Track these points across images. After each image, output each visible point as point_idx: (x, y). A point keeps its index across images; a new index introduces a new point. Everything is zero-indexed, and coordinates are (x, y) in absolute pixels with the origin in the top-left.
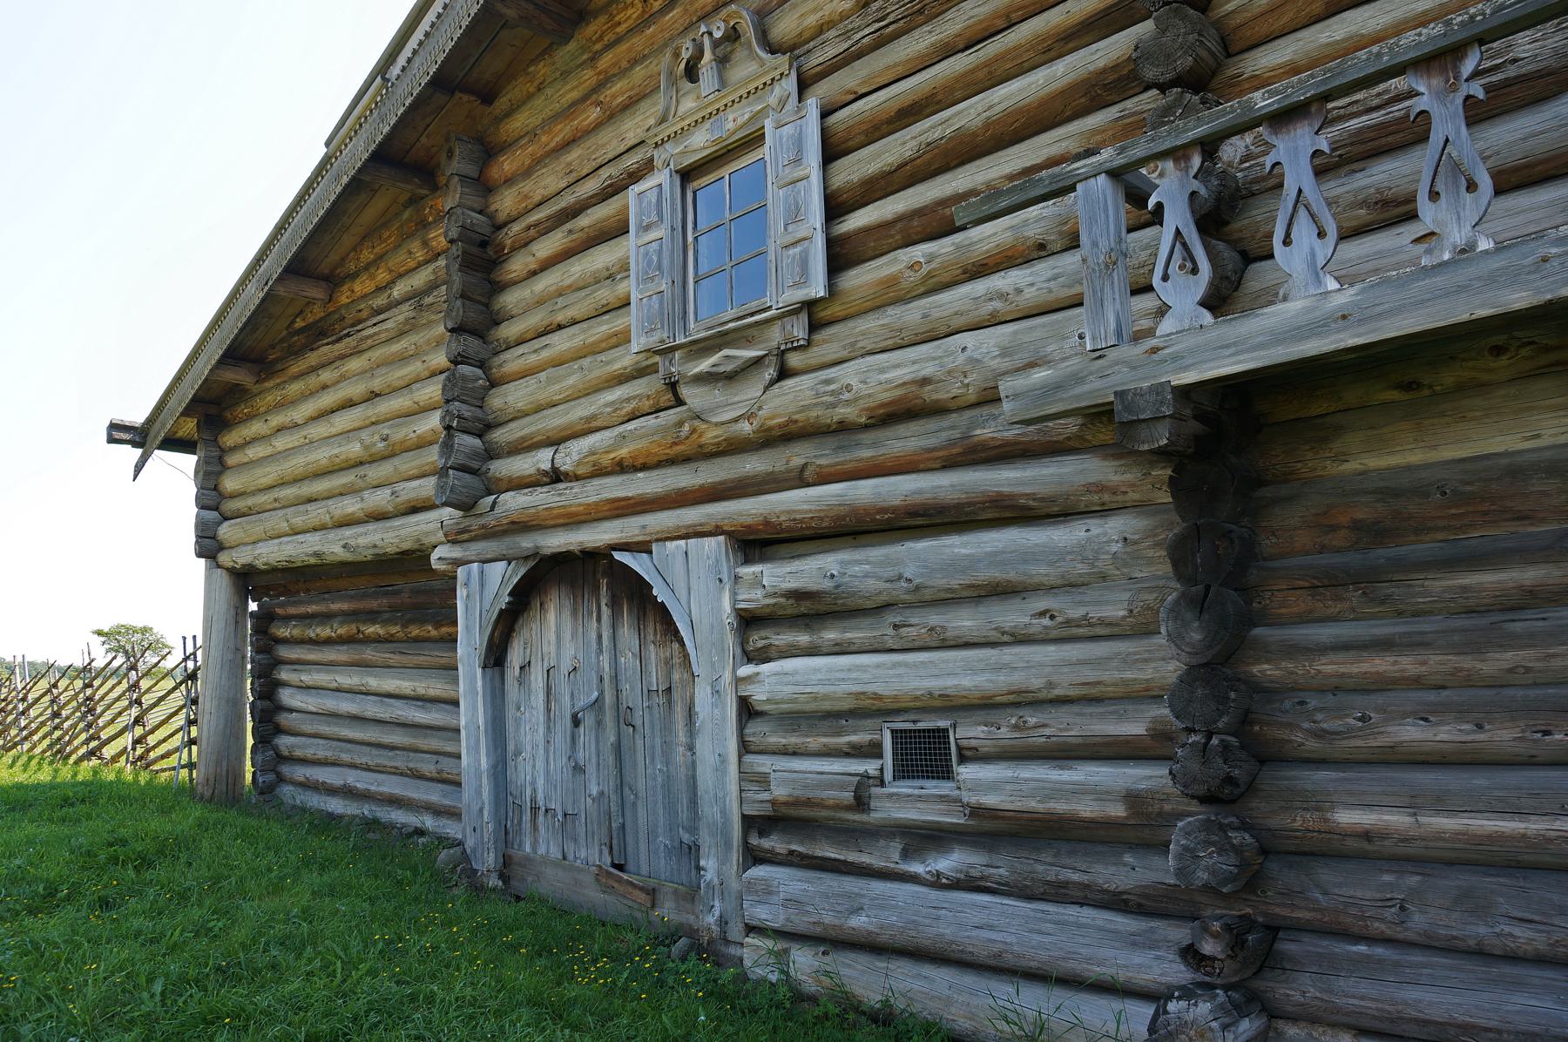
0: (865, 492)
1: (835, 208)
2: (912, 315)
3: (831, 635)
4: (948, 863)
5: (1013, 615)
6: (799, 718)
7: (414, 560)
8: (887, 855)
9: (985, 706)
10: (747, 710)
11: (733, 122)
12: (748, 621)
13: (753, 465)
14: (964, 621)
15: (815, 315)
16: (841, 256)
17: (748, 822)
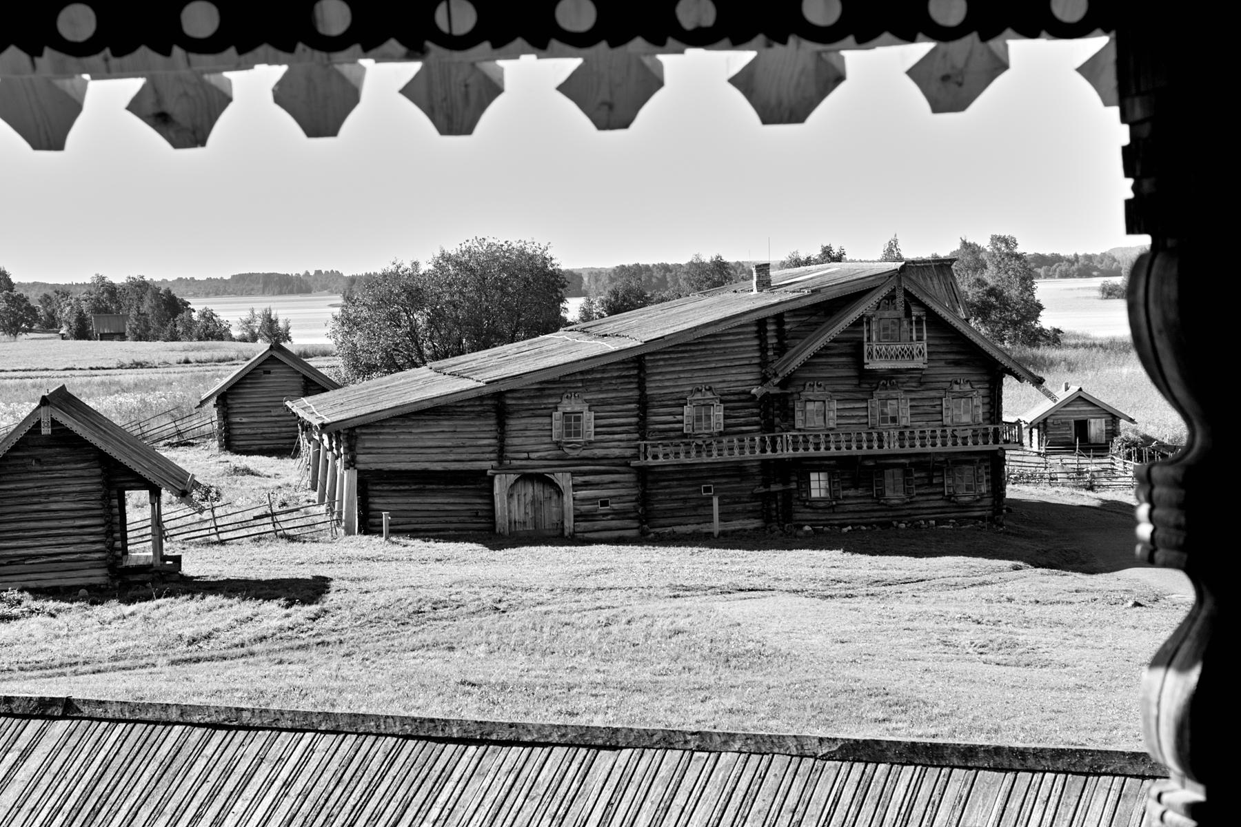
0: (598, 468)
1: (595, 427)
2: (606, 445)
4: (609, 517)
5: (618, 485)
6: (583, 500)
8: (601, 517)
9: (614, 497)
10: (574, 499)
11: (577, 409)
12: (574, 485)
13: (579, 462)
14: (611, 486)
15: (590, 442)
16: (596, 434)
17: (575, 516)
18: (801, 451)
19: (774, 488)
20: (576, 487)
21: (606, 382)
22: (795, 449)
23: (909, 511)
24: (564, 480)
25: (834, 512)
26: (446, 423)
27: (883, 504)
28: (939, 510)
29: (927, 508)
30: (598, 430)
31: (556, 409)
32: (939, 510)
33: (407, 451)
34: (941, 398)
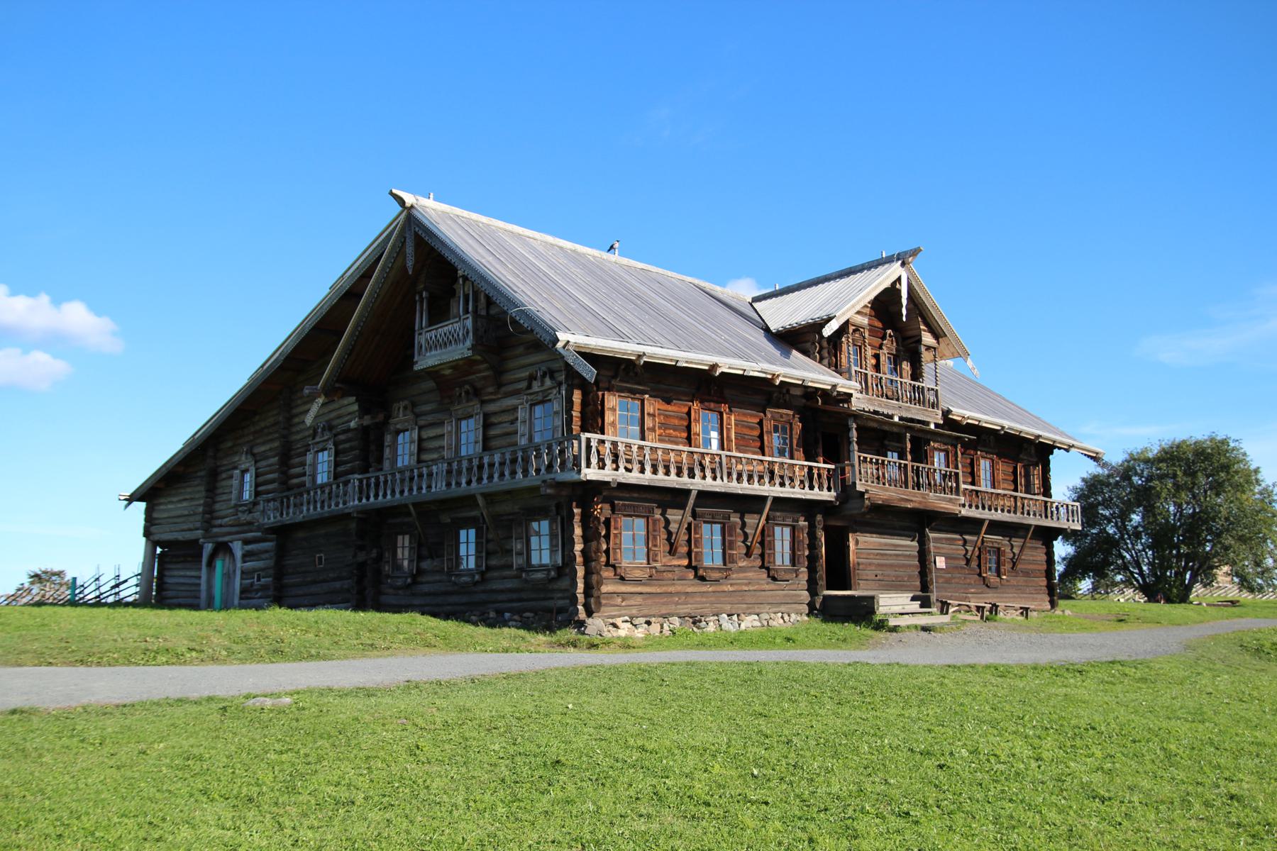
3: (252, 558)
7: (196, 541)
18: (364, 501)
19: (361, 557)
20: (247, 556)
21: (266, 431)
22: (360, 500)
23: (484, 597)
24: (238, 548)
25: (413, 595)
26: (189, 490)
27: (455, 584)
28: (515, 596)
29: (502, 591)
30: (260, 489)
31: (236, 468)
32: (515, 596)
33: (171, 520)
34: (515, 409)
